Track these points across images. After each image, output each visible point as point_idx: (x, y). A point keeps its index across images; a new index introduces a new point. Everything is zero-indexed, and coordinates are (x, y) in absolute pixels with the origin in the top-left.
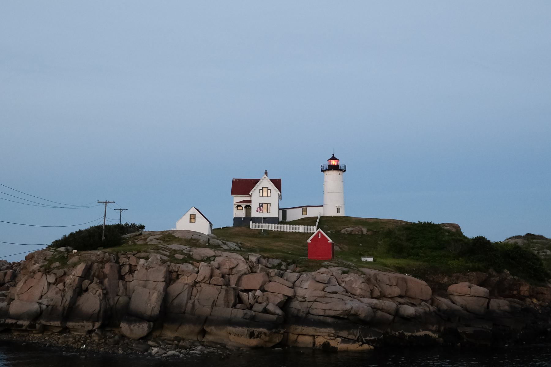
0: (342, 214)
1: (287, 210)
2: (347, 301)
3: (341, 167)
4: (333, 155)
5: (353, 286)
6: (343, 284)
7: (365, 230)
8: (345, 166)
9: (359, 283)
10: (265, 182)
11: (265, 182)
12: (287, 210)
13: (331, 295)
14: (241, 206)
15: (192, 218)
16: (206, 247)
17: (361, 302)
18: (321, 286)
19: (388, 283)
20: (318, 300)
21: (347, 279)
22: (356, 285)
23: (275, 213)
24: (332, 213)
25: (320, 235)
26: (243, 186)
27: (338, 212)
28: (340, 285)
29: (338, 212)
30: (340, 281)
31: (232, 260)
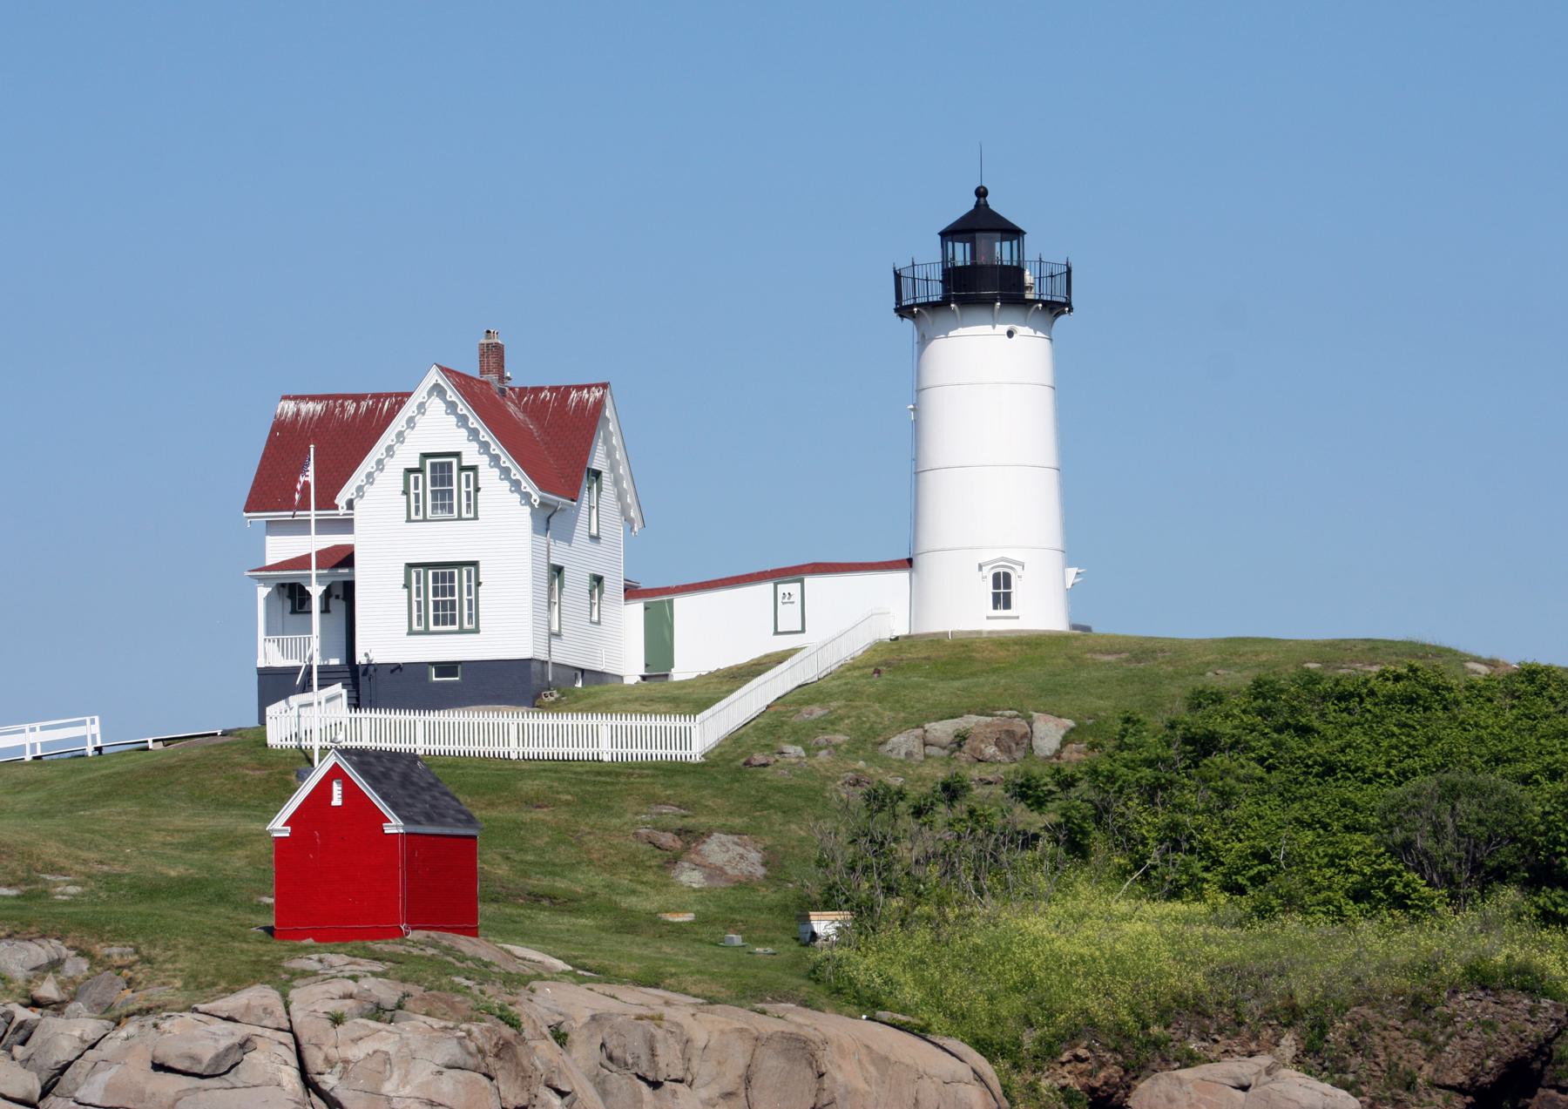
0: (1040, 610)
4: (981, 193)
5: (388, 1088)
6: (329, 1081)
7: (1048, 733)
9: (422, 1072)
10: (433, 425)
11: (433, 425)
12: (682, 604)
19: (644, 1068)
21: (357, 1052)
22: (405, 1080)
23: (505, 629)
24: (964, 611)
26: (315, 452)
27: (1002, 599)
28: (308, 1081)
29: (1002, 599)
30: (315, 1060)
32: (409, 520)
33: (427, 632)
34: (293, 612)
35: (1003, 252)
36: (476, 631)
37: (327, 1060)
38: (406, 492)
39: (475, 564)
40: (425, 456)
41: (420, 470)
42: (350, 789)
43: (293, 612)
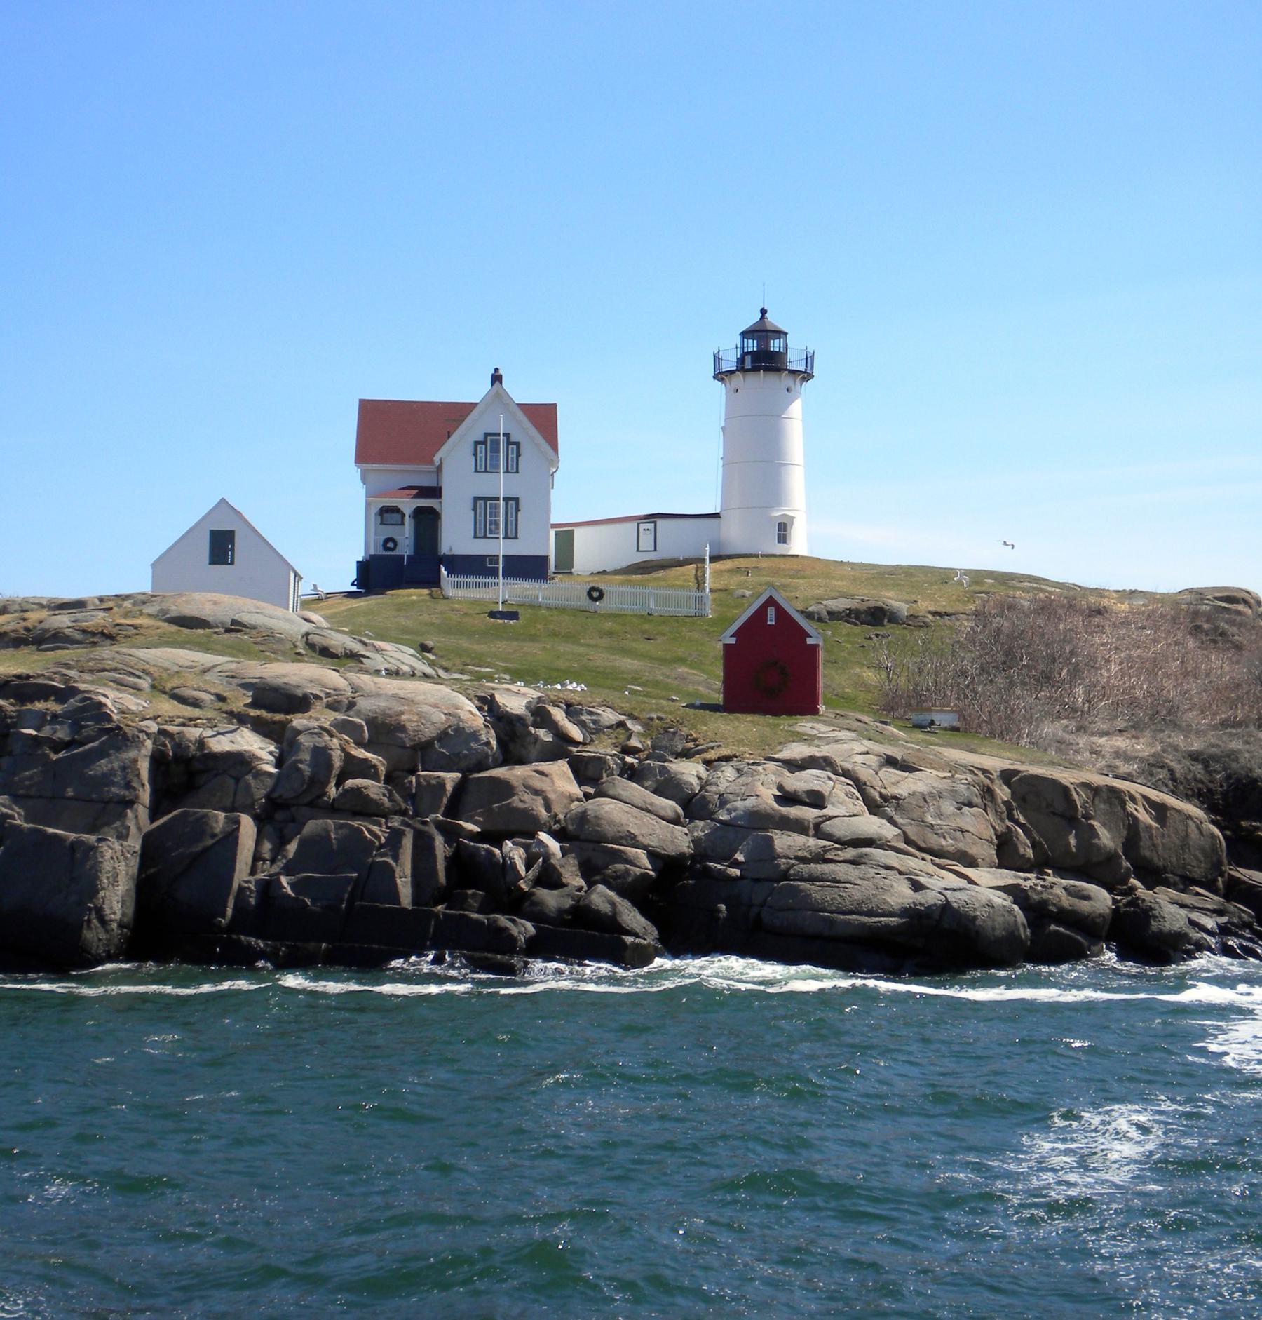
0: (799, 545)
1: (579, 533)
2: (923, 880)
3: (795, 361)
4: (763, 312)
5: (929, 819)
8: (809, 359)
9: (949, 807)
13: (850, 853)
14: (395, 510)
15: (221, 546)
16: (298, 657)
17: (971, 882)
18: (810, 814)
19: (1060, 806)
20: (802, 868)
21: (901, 791)
25: (771, 611)
27: (783, 537)
31: (425, 708)
32: (476, 471)
33: (485, 537)
34: (382, 523)
35: (775, 345)
36: (516, 537)
37: (881, 795)
38: (475, 455)
39: (516, 500)
40: (487, 435)
41: (484, 443)
42: (781, 613)
43: (382, 523)
